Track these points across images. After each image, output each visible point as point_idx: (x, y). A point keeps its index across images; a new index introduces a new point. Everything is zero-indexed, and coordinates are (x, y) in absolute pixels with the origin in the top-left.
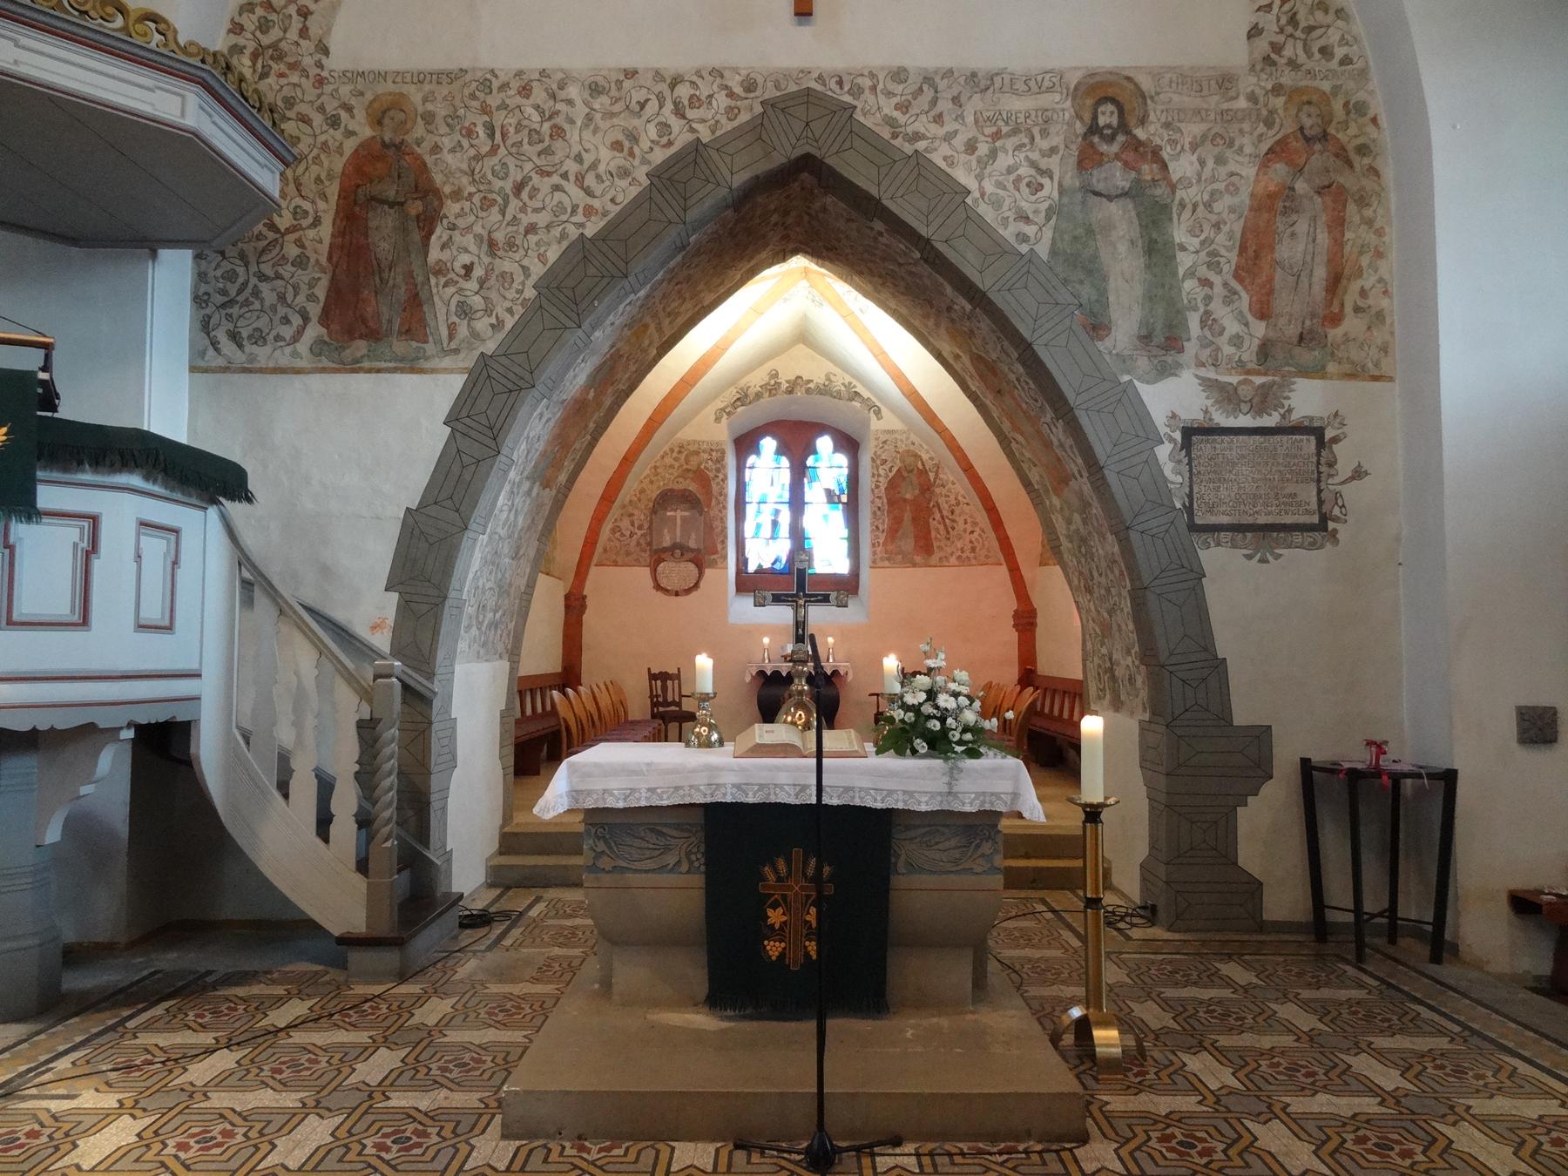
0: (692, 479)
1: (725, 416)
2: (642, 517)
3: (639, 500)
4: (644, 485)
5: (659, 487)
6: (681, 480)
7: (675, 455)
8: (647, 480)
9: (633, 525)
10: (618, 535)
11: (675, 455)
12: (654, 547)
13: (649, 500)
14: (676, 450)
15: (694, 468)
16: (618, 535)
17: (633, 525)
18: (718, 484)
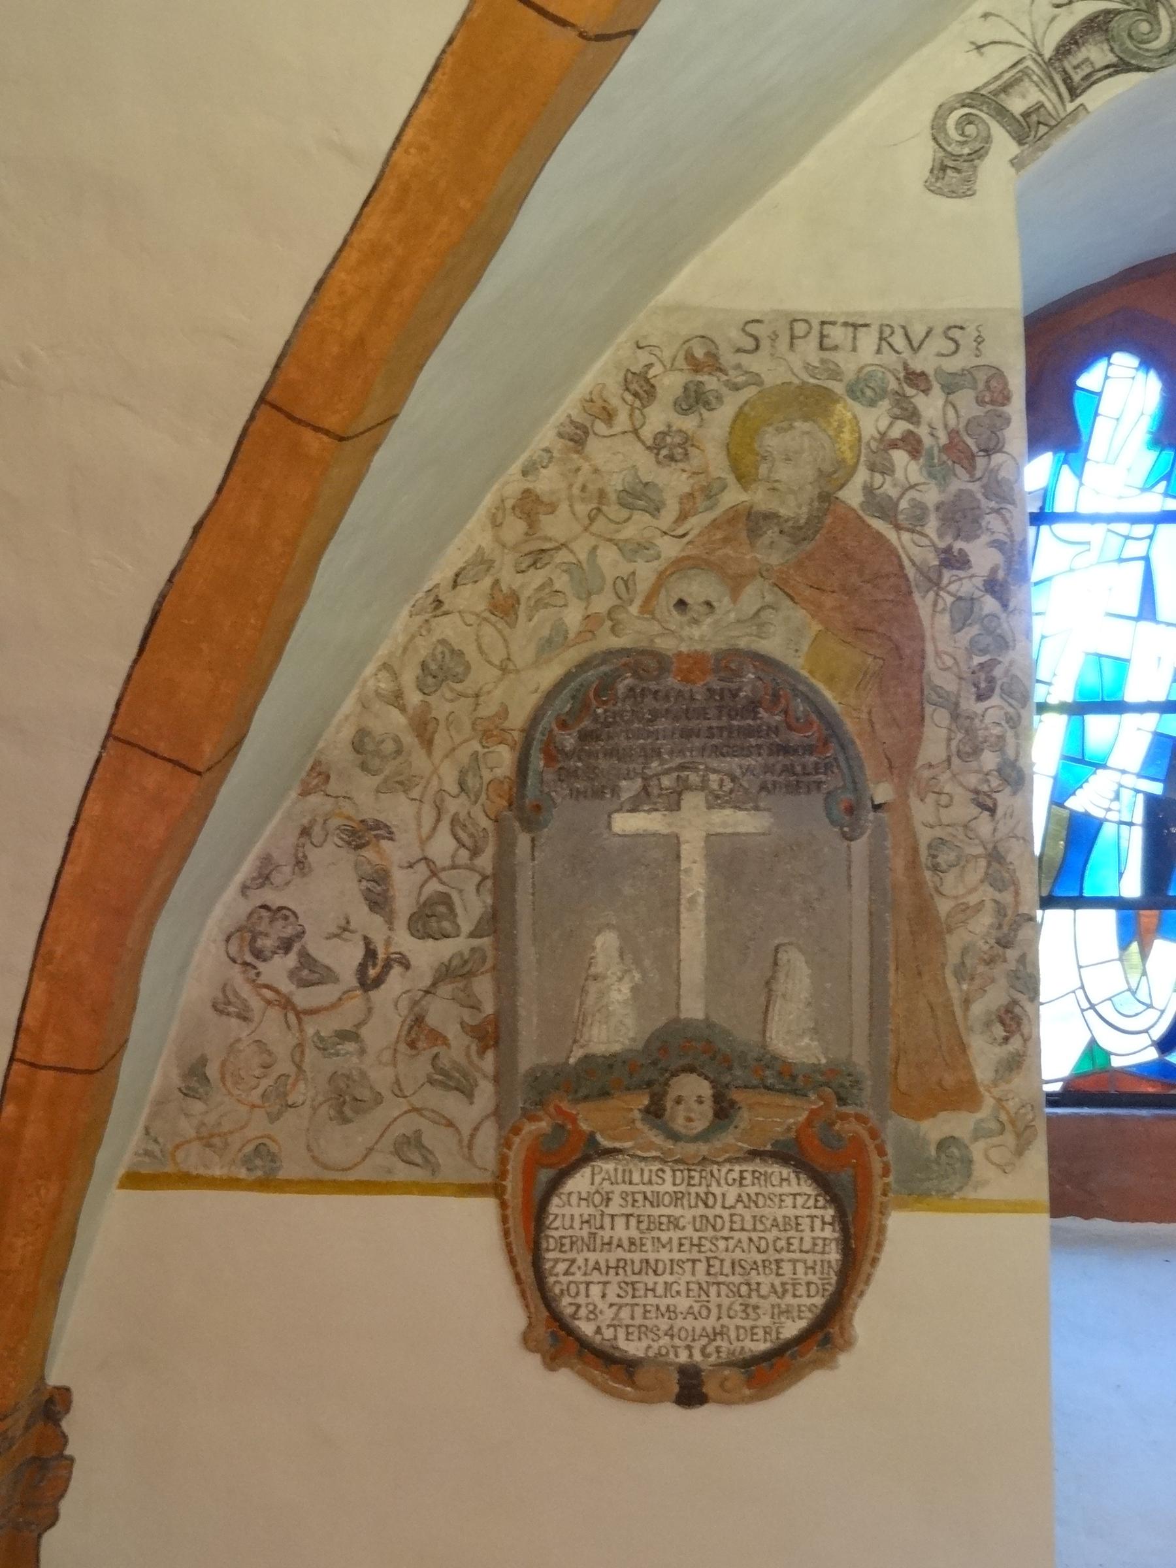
0: (782, 585)
1: (1003, 145)
2: (443, 846)
3: (424, 728)
4: (447, 628)
5: (549, 646)
6: (697, 588)
7: (657, 418)
8: (472, 597)
9: (379, 902)
10: (278, 970)
11: (657, 418)
12: (528, 1058)
13: (490, 732)
14: (671, 383)
15: (793, 508)
16: (278, 970)
17: (379, 902)
18: (964, 612)
